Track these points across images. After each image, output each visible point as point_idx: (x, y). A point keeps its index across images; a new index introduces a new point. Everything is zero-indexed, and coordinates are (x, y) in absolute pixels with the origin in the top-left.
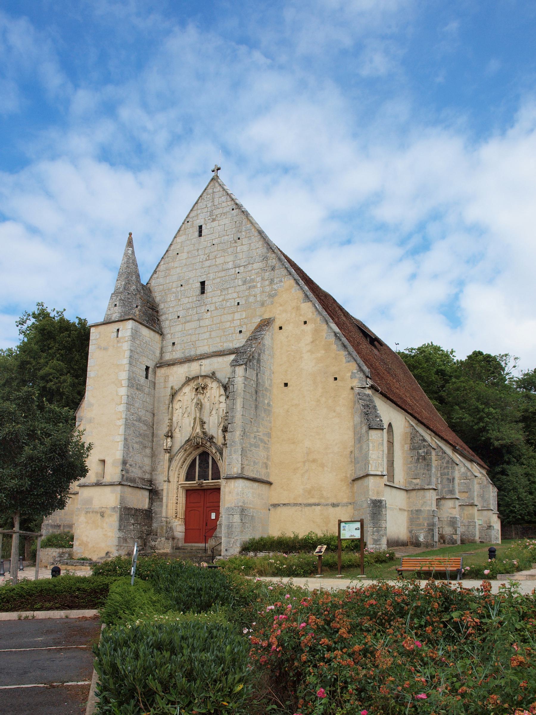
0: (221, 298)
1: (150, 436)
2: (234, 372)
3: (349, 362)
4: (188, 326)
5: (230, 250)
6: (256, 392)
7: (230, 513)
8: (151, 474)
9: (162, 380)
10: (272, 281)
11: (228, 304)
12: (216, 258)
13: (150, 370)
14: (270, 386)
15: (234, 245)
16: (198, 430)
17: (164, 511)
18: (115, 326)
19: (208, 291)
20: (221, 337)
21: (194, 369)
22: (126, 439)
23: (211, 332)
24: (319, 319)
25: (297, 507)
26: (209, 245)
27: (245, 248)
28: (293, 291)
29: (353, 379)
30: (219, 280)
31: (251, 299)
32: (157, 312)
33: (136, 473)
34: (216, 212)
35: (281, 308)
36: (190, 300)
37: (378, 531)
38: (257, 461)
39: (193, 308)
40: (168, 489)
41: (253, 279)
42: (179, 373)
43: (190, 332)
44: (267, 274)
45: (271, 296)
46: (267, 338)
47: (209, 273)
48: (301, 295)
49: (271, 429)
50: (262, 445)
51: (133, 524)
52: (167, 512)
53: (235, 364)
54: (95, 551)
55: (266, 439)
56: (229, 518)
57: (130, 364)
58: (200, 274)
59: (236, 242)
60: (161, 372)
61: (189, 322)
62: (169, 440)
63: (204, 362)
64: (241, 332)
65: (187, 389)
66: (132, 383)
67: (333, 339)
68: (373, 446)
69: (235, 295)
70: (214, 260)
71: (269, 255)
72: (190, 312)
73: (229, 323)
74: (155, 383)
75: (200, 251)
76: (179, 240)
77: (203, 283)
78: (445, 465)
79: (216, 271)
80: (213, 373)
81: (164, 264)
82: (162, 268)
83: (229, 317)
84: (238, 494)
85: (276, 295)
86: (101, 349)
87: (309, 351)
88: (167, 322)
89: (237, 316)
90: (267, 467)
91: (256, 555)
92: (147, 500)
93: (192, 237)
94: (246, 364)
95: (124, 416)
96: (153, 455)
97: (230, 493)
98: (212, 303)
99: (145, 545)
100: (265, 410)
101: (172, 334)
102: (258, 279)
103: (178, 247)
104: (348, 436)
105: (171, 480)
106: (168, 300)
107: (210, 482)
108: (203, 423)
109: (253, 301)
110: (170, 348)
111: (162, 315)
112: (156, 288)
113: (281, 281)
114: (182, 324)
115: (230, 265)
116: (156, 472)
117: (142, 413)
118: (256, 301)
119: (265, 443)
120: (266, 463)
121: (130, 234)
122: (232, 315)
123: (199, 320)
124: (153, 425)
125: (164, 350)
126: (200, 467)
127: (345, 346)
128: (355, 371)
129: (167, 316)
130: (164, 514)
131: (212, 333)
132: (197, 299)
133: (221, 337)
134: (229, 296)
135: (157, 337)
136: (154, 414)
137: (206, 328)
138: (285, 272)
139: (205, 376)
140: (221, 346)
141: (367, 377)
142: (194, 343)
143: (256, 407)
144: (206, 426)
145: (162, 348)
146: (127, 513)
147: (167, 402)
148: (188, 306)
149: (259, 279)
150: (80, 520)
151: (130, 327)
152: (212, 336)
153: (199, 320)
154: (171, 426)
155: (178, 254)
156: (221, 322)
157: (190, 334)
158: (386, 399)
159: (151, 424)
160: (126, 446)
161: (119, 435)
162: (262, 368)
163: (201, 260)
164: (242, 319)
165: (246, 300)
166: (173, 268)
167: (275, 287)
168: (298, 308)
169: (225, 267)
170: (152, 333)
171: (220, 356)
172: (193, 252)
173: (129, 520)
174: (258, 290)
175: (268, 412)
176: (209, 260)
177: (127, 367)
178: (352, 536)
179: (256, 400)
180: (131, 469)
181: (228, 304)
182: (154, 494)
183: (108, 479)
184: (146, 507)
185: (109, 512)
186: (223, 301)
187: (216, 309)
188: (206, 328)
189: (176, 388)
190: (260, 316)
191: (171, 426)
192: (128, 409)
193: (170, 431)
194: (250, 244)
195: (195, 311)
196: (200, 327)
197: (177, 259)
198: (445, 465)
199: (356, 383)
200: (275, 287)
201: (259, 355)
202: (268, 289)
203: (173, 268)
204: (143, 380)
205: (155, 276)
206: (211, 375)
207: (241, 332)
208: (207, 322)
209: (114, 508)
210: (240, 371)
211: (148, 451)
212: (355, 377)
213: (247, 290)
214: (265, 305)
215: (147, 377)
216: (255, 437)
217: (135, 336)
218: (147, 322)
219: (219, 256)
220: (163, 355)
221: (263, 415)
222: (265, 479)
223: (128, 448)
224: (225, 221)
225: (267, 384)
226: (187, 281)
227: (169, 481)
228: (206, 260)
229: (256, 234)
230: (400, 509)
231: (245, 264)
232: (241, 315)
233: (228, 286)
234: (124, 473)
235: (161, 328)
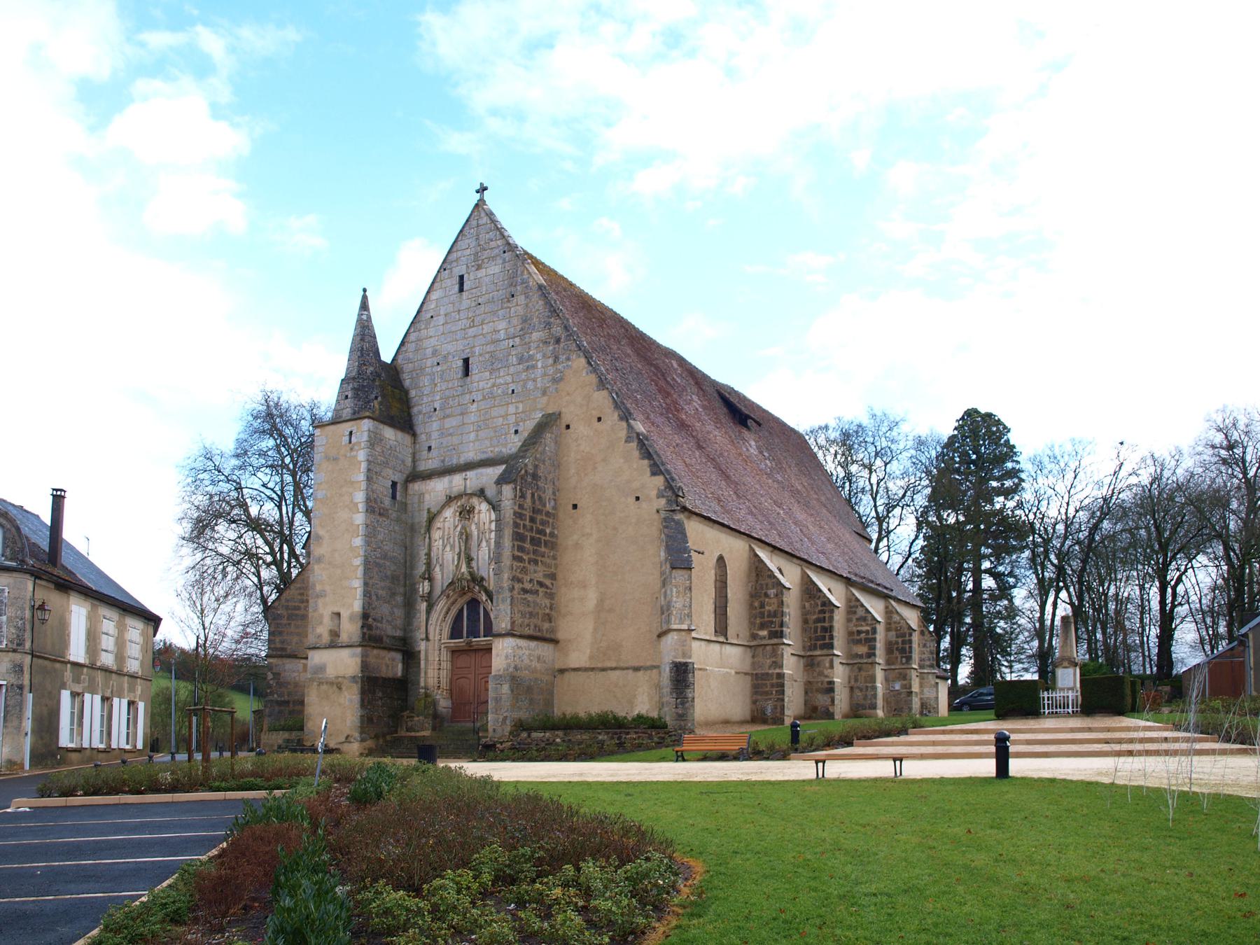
1: (401, 578)
2: (500, 492)
5: (501, 313)
16: (464, 569)
17: (422, 680)
18: (346, 427)
21: (457, 482)
22: (366, 584)
31: (530, 385)
34: (486, 254)
37: (683, 704)
40: (426, 651)
42: (437, 489)
45: (556, 381)
49: (556, 566)
52: (426, 682)
53: (501, 481)
55: (548, 582)
57: (369, 479)
60: (416, 486)
61: (448, 416)
63: (470, 474)
65: (449, 513)
66: (373, 507)
68: (678, 592)
69: (509, 379)
74: (406, 504)
76: (434, 296)
82: (412, 337)
83: (502, 411)
84: (507, 657)
85: (561, 379)
89: (512, 409)
92: (400, 666)
95: (362, 553)
104: (654, 579)
105: (431, 637)
108: (469, 560)
113: (568, 359)
115: (502, 335)
117: (388, 547)
118: (536, 388)
121: (365, 290)
123: (462, 414)
130: (422, 684)
134: (498, 381)
135: (407, 439)
144: (474, 564)
145: (414, 454)
146: (371, 684)
149: (539, 356)
151: (366, 428)
160: (367, 594)
165: (524, 386)
167: (560, 367)
170: (400, 434)
173: (374, 692)
174: (539, 372)
177: (363, 486)
182: (410, 657)
187: (484, 398)
190: (542, 409)
192: (368, 543)
200: (560, 367)
202: (551, 371)
204: (387, 501)
205: (404, 349)
207: (516, 432)
210: (507, 490)
211: (399, 599)
215: (394, 497)
216: (531, 581)
223: (370, 597)
224: (495, 269)
227: (427, 639)
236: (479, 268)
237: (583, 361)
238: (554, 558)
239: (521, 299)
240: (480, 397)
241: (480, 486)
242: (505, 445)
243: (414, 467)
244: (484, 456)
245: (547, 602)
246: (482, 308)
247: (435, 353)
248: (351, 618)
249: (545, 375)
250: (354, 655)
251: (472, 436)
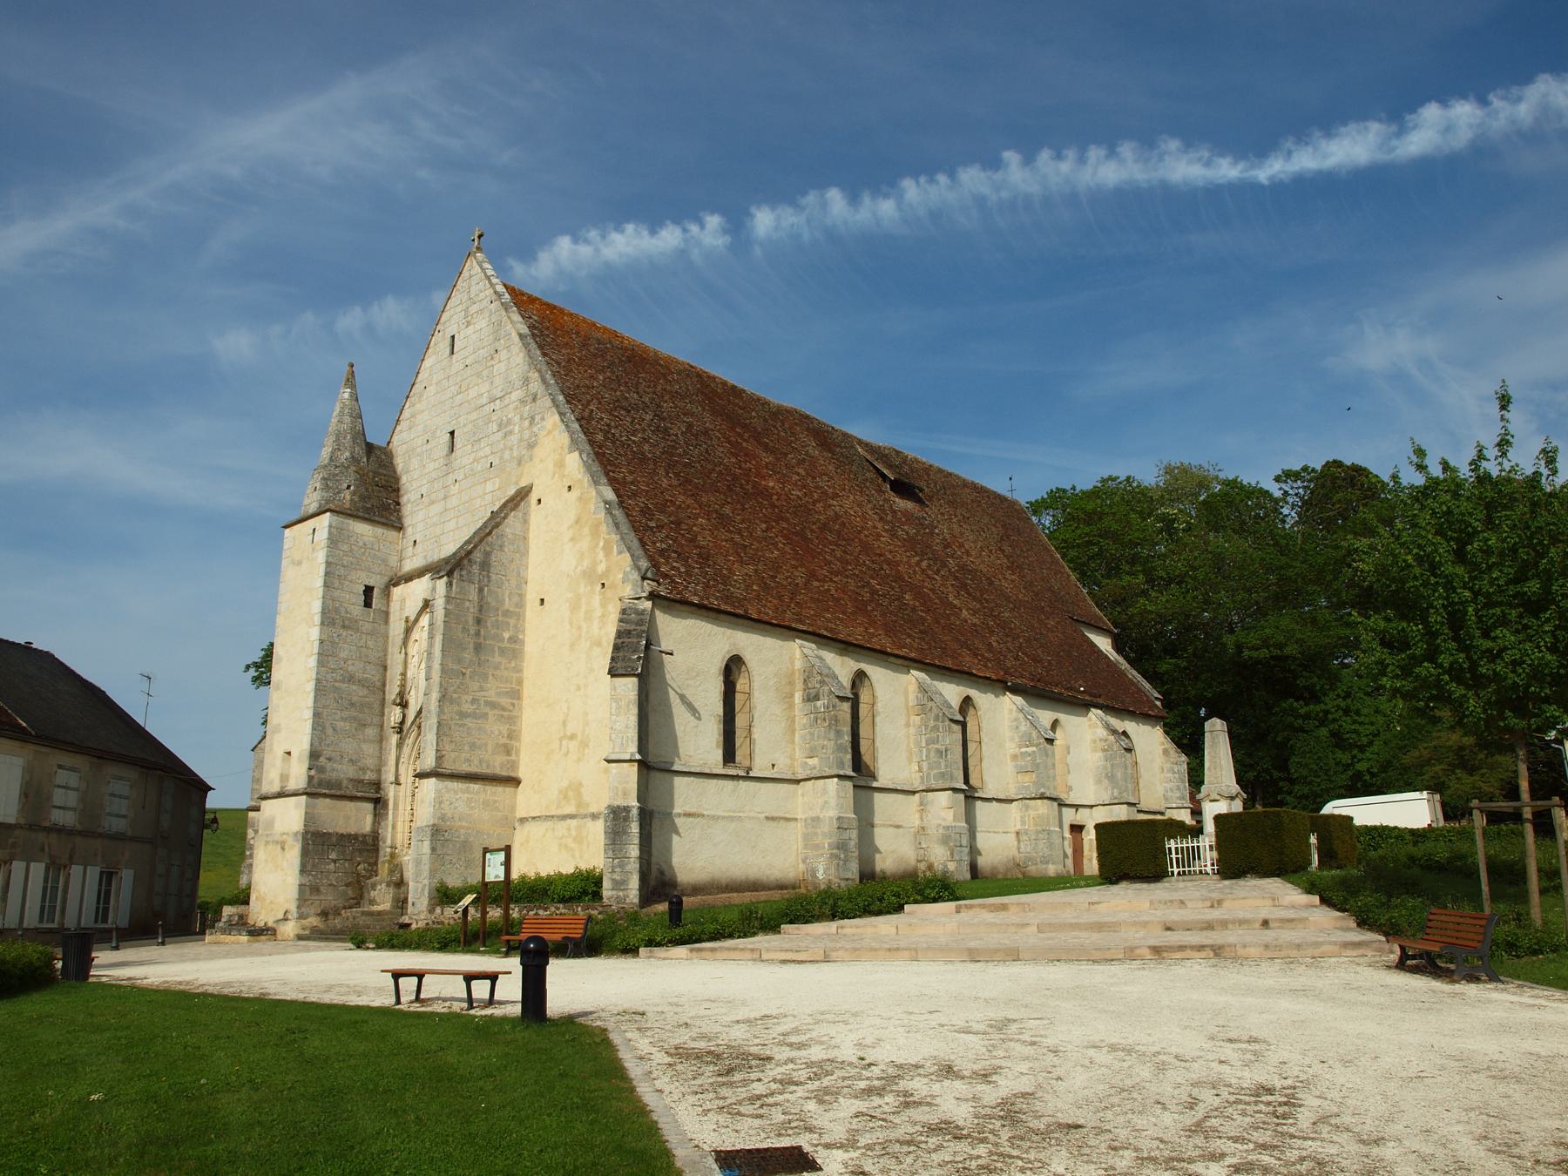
0: (472, 458)
6: (478, 621)
8: (379, 772)
10: (533, 418)
13: (376, 592)
14: (521, 604)
22: (316, 715)
24: (586, 479)
28: (556, 433)
32: (398, 490)
33: (343, 771)
38: (478, 743)
46: (511, 525)
48: (565, 439)
49: (520, 682)
50: (491, 713)
51: (335, 861)
55: (505, 701)
57: (326, 585)
60: (396, 592)
62: (398, 710)
66: (331, 617)
67: (602, 515)
68: (619, 708)
74: (387, 614)
78: (932, 723)
87: (572, 539)
89: (489, 487)
90: (508, 753)
92: (369, 819)
94: (450, 574)
96: (381, 739)
99: (361, 896)
100: (502, 651)
105: (402, 780)
117: (355, 668)
119: (504, 709)
120: (505, 745)
124: (384, 685)
127: (617, 525)
130: (389, 842)
135: (392, 534)
136: (385, 668)
138: (548, 402)
141: (644, 578)
143: (478, 648)
148: (434, 475)
149: (517, 419)
153: (445, 498)
154: (403, 686)
157: (434, 525)
158: (712, 614)
159: (378, 684)
162: (493, 577)
167: (535, 429)
168: (560, 464)
170: (379, 530)
174: (514, 439)
175: (514, 651)
179: (478, 634)
180: (329, 765)
182: (379, 803)
184: (367, 826)
191: (403, 686)
192: (321, 662)
193: (401, 694)
198: (932, 723)
199: (628, 591)
201: (487, 554)
204: (357, 609)
211: (371, 732)
215: (368, 604)
216: (474, 701)
217: (334, 541)
218: (367, 510)
221: (497, 659)
222: (504, 774)
225: (508, 605)
230: (767, 818)
234: (313, 773)
235: (400, 519)
237: (557, 417)
238: (519, 670)
239: (503, 354)
245: (504, 729)
249: (521, 440)
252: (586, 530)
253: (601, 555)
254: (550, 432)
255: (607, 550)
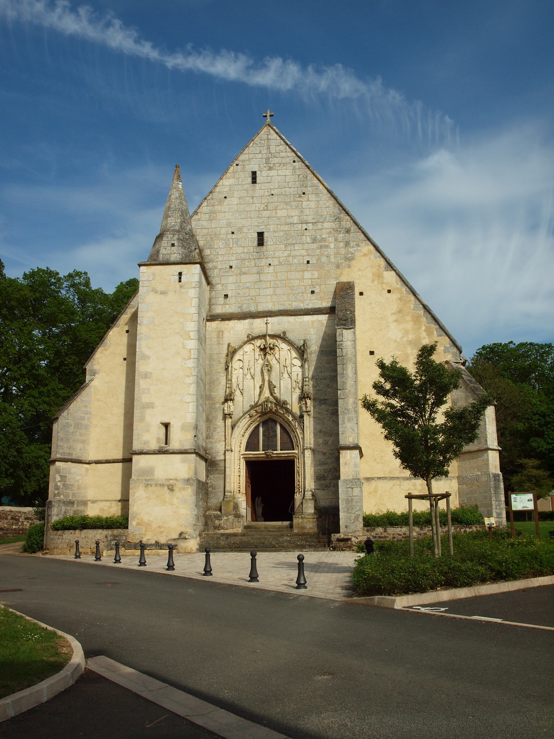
0: (286, 253)
3: (440, 336)
4: (244, 278)
5: (293, 204)
7: (348, 486)
9: (214, 335)
10: (347, 244)
11: (295, 261)
12: (276, 209)
15: (298, 199)
16: (266, 393)
19: (269, 243)
20: (288, 295)
21: (258, 326)
23: (275, 288)
25: (395, 481)
26: (266, 194)
27: (313, 205)
28: (372, 257)
29: (447, 354)
30: (282, 233)
31: (324, 259)
35: (360, 273)
36: (246, 250)
39: (250, 259)
41: (324, 238)
43: (248, 285)
44: (342, 235)
45: (347, 259)
47: (269, 225)
54: (162, 532)
56: (347, 491)
58: (256, 224)
59: (300, 197)
61: (245, 273)
64: (313, 292)
65: (248, 348)
69: (304, 252)
70: (275, 211)
71: (342, 216)
72: (247, 263)
73: (298, 282)
75: (255, 199)
77: (261, 235)
79: (278, 223)
80: (284, 333)
81: (207, 206)
83: (298, 275)
85: (353, 259)
86: (156, 292)
87: (396, 321)
88: (216, 271)
89: (307, 275)
91: (385, 531)
93: (244, 183)
95: (194, 373)
97: (346, 464)
98: (275, 257)
101: (223, 285)
102: (330, 239)
103: (226, 190)
106: (216, 247)
107: (279, 452)
109: (326, 261)
110: (221, 300)
111: (208, 262)
112: (198, 231)
113: (358, 245)
114: (237, 275)
116: (211, 440)
122: (301, 273)
123: (258, 273)
125: (213, 301)
126: (264, 435)
128: (448, 346)
129: (215, 264)
131: (277, 289)
132: (255, 250)
133: (288, 295)
137: (269, 283)
139: (273, 336)
140: (289, 304)
142: (254, 298)
147: (223, 361)
148: (243, 256)
149: (331, 239)
150: (137, 495)
152: (277, 293)
155: (225, 197)
156: (288, 279)
161: (189, 394)
163: (257, 209)
164: (315, 279)
165: (318, 260)
166: (220, 212)
167: (351, 250)
168: (379, 276)
169: (291, 220)
171: (291, 315)
172: (247, 198)
176: (267, 210)
178: (524, 507)
181: (295, 261)
183: (175, 444)
185: (179, 485)
186: (289, 256)
187: (280, 264)
188: (269, 283)
189: (234, 345)
194: (318, 201)
195: (253, 262)
196: (260, 281)
197: (225, 204)
200: (351, 250)
202: (343, 251)
203: (220, 212)
206: (282, 335)
207: (313, 292)
208: (269, 277)
209: (188, 480)
212: (449, 352)
213: (318, 248)
214: (341, 267)
219: (279, 208)
220: (213, 307)
226: (240, 229)
228: (264, 210)
229: (325, 191)
231: (314, 221)
232: (312, 274)
233: (294, 242)
236: (270, 169)
240: (276, 262)
241: (283, 330)
242: (303, 301)
243: (210, 310)
244: (281, 308)
246: (275, 198)
247: (229, 225)
248: (184, 428)
250: (183, 461)
251: (270, 291)
252: (409, 318)
253: (424, 334)
254: (365, 255)
255: (429, 332)
